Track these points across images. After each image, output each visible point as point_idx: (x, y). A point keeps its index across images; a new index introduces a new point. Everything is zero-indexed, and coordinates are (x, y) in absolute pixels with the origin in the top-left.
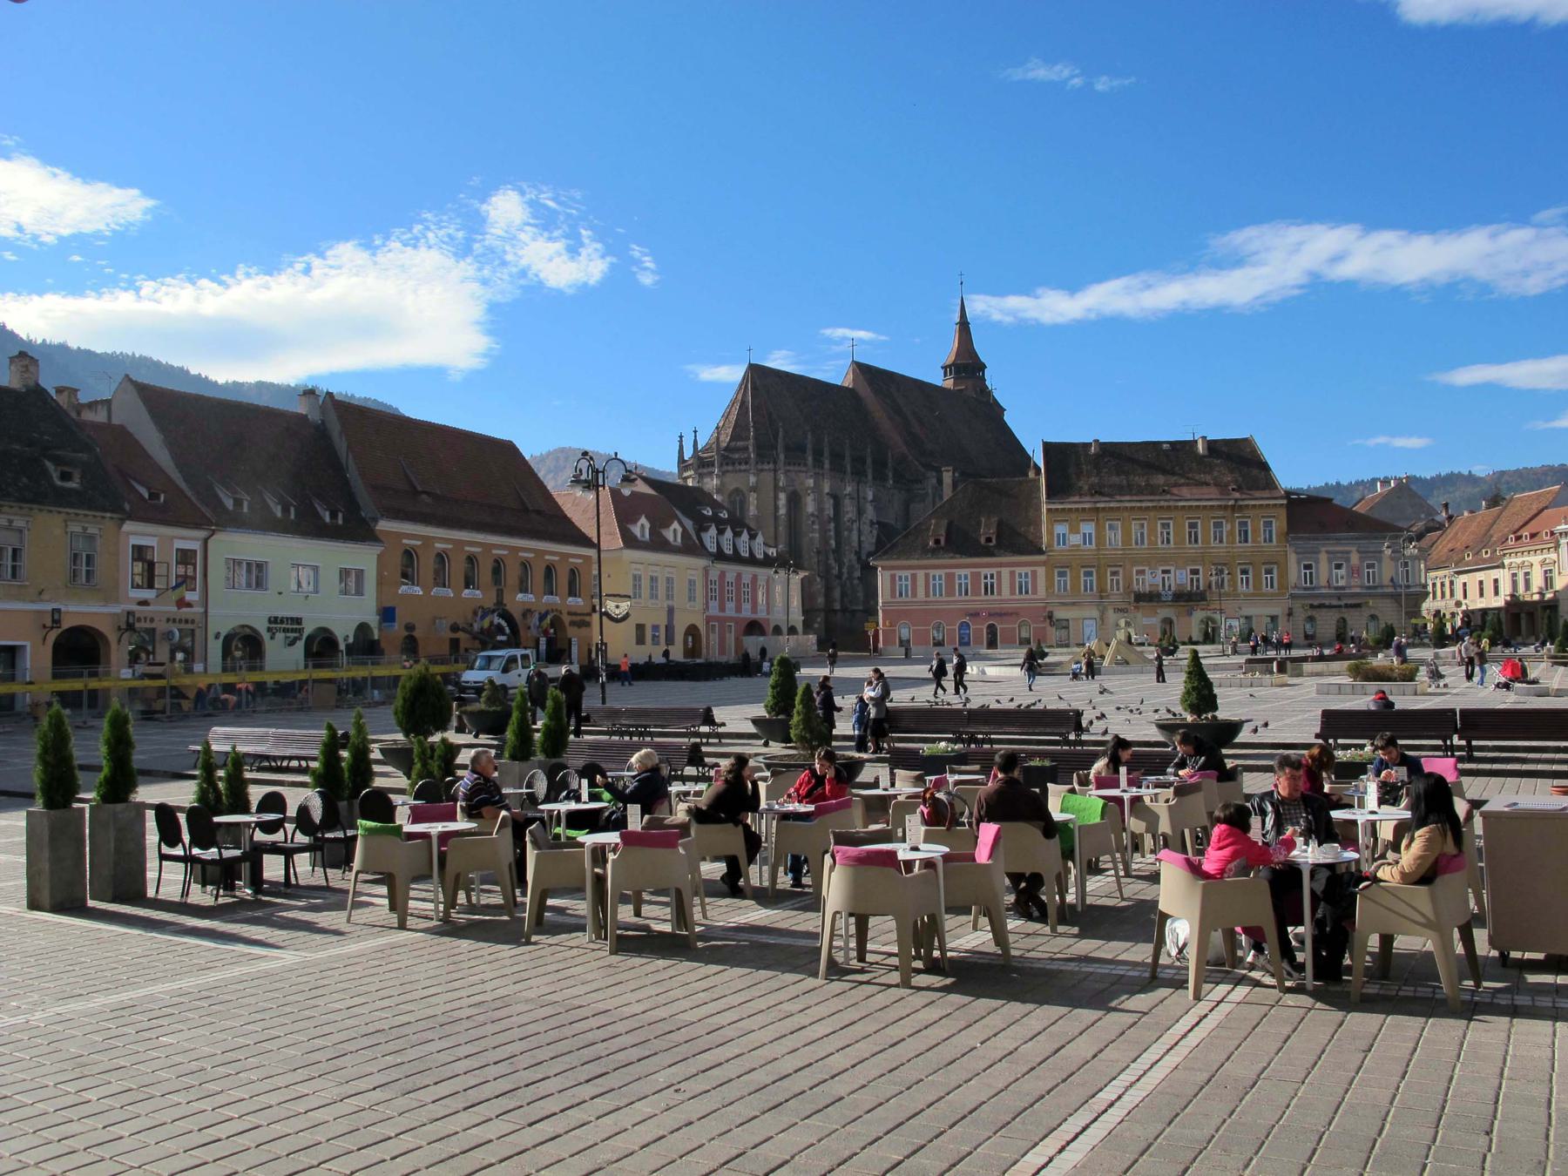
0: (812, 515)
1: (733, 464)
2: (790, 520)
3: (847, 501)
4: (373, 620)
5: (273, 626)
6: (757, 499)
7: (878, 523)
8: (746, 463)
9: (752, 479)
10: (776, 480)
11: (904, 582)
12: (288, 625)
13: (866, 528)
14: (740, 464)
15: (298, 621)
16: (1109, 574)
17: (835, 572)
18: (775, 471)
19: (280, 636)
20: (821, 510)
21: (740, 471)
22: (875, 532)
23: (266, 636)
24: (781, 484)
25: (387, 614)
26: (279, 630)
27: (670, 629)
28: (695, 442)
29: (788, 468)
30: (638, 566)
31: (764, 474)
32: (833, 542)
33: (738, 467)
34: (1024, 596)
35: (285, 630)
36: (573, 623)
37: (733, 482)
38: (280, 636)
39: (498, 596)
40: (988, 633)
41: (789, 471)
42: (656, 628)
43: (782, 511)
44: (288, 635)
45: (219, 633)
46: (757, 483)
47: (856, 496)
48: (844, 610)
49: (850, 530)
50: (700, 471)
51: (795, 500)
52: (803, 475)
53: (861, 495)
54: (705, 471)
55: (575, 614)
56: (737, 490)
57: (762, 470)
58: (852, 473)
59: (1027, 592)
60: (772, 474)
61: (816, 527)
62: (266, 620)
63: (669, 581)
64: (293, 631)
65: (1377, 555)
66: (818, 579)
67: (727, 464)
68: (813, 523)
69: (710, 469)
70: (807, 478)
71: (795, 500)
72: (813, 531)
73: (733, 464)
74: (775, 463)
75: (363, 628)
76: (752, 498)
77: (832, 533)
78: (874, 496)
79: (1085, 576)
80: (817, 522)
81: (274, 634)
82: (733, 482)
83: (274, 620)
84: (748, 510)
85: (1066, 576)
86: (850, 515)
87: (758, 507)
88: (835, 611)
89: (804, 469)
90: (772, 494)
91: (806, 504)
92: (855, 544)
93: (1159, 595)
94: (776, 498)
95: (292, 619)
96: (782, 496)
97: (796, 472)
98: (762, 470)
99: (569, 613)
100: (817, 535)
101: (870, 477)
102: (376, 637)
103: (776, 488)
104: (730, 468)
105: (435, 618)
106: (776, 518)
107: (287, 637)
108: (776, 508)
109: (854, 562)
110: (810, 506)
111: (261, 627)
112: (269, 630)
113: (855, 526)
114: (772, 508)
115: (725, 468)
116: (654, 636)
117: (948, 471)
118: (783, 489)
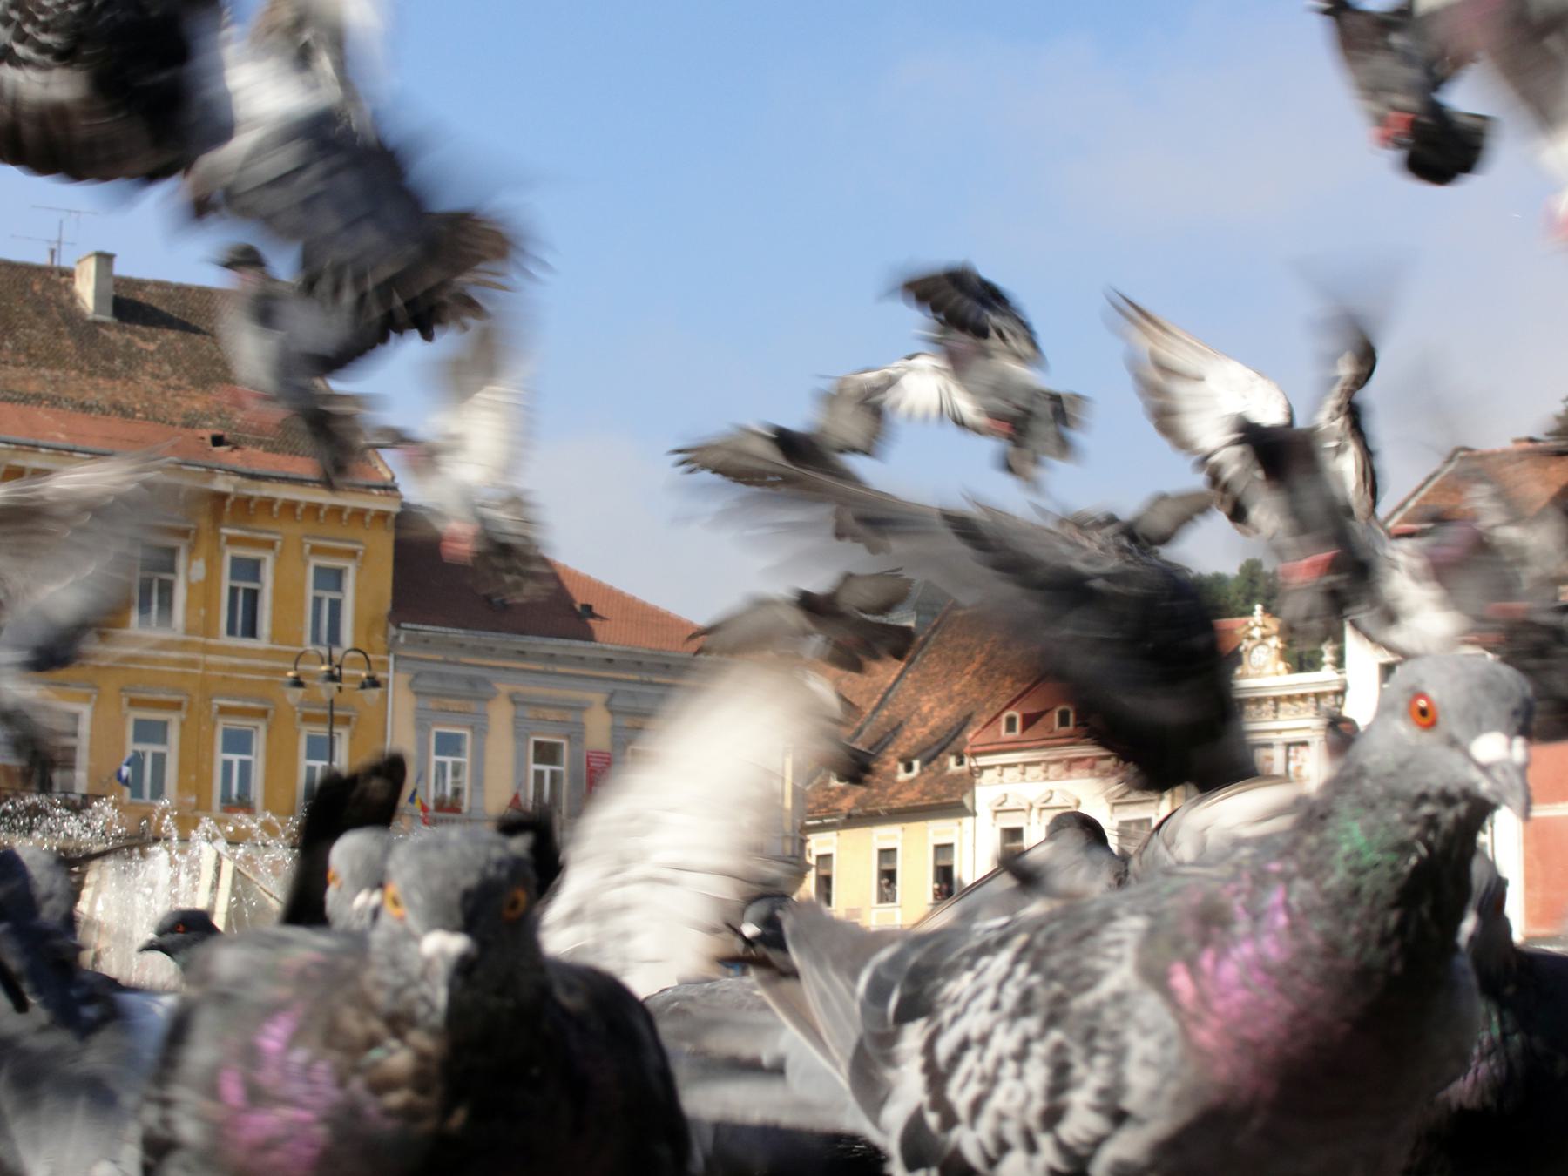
65: (571, 716)
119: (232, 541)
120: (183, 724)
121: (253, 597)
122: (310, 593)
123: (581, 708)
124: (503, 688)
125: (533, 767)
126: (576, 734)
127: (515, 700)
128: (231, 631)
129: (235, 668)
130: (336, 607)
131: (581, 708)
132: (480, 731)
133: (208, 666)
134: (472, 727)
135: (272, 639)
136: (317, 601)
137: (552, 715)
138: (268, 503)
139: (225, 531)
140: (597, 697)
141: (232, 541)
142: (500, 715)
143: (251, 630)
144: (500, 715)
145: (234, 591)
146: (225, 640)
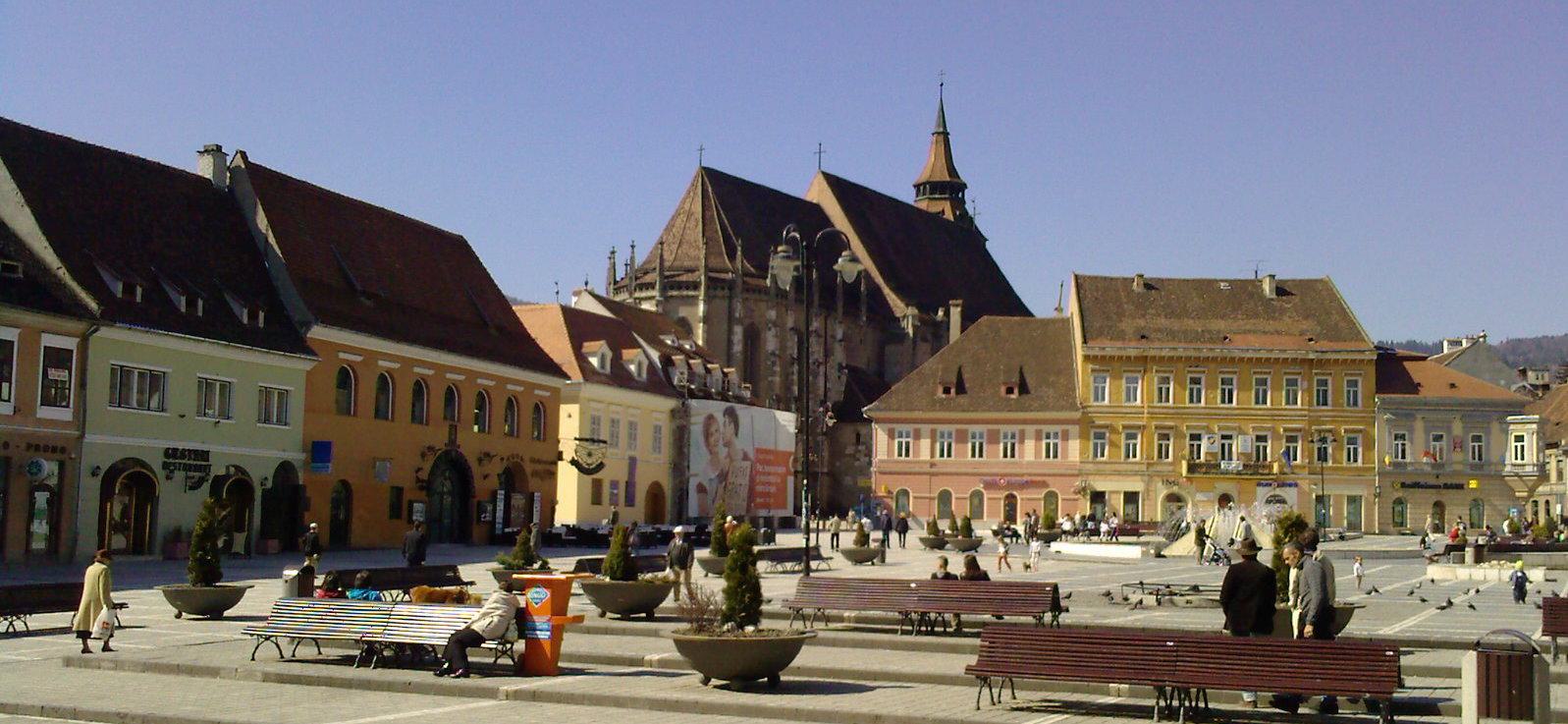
0: (773, 354)
2: (746, 358)
3: (813, 340)
4: (296, 456)
5: (171, 460)
7: (847, 367)
10: (731, 311)
12: (190, 463)
13: (833, 373)
15: (204, 455)
16: (1156, 437)
18: (730, 298)
19: (179, 475)
20: (783, 347)
22: (844, 378)
23: (161, 473)
24: (737, 315)
25: (320, 451)
26: (178, 467)
27: (630, 485)
29: (747, 296)
30: (619, 409)
31: (717, 301)
32: (796, 388)
33: (685, 293)
35: (187, 468)
36: (535, 474)
38: (179, 475)
39: (450, 434)
40: (1005, 506)
41: (747, 298)
42: (614, 485)
44: (191, 474)
45: (98, 467)
47: (822, 333)
49: (816, 377)
51: (753, 337)
52: (763, 305)
53: (829, 333)
55: (539, 461)
57: (715, 297)
58: (820, 306)
60: (726, 303)
61: (777, 369)
62: (162, 454)
63: (632, 425)
64: (198, 468)
68: (774, 364)
70: (768, 308)
71: (753, 337)
72: (774, 374)
75: (285, 469)
77: (795, 377)
78: (844, 333)
80: (778, 363)
81: (172, 472)
83: (171, 453)
85: (1136, 438)
86: (816, 356)
89: (765, 298)
90: (725, 326)
91: (765, 342)
92: (821, 391)
94: (730, 332)
95: (196, 452)
96: (738, 330)
97: (756, 300)
99: (533, 461)
100: (777, 379)
101: (840, 310)
102: (301, 483)
103: (731, 320)
105: (375, 460)
107: (187, 478)
108: (730, 343)
110: (770, 342)
111: (156, 462)
112: (165, 466)
113: (822, 369)
114: (724, 344)
116: (612, 494)
117: (957, 306)
118: (740, 321)
119: (1316, 374)
122: (1345, 389)
124: (1419, 416)
128: (1318, 404)
130: (1355, 393)
132: (1411, 430)
136: (1349, 392)
141: (1316, 374)
142: (1419, 425)
143: (1326, 404)
144: (1419, 425)
145: (1318, 391)
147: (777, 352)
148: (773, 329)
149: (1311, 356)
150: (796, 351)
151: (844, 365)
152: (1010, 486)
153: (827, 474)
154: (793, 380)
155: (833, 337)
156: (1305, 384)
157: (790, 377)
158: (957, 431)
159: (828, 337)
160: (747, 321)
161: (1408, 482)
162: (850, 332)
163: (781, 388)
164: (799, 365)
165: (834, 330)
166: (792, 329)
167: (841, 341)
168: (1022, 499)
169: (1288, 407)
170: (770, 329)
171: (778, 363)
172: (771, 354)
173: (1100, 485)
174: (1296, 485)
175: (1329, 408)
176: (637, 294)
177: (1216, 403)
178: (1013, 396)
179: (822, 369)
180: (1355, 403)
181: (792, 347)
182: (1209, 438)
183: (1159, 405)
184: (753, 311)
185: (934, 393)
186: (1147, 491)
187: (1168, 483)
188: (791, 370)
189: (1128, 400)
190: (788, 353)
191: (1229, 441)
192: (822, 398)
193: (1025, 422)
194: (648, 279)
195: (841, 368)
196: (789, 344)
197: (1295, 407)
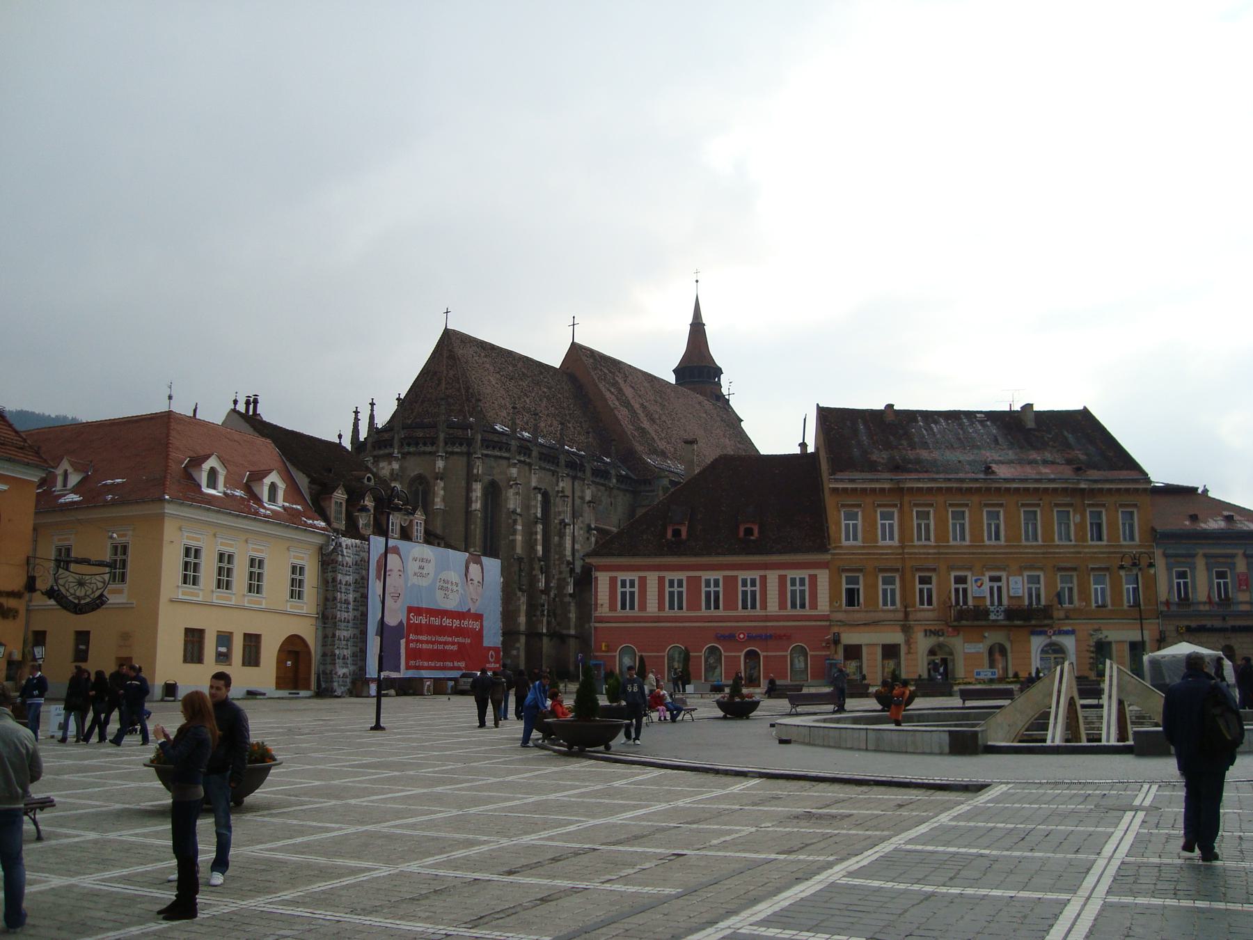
0: (514, 512)
1: (417, 444)
6: (444, 489)
8: (433, 444)
9: (440, 464)
11: (676, 589)
14: (425, 444)
17: (542, 585)
18: (469, 454)
21: (424, 453)
28: (372, 417)
32: (540, 548)
33: (423, 449)
34: (799, 612)
37: (415, 467)
43: (477, 506)
46: (445, 468)
48: (552, 635)
50: (375, 453)
51: (493, 492)
52: (504, 463)
54: (381, 452)
56: (420, 478)
57: (452, 453)
59: (803, 606)
65: (1229, 560)
66: (519, 594)
67: (409, 445)
69: (387, 451)
71: (493, 492)
73: (417, 444)
74: (469, 445)
76: (439, 489)
77: (539, 537)
79: (884, 583)
82: (415, 467)
84: (433, 503)
85: (893, 583)
87: (444, 499)
88: (540, 635)
91: (507, 499)
93: (986, 613)
94: (469, 490)
98: (452, 453)
104: (412, 449)
106: (468, 513)
108: (468, 501)
109: (566, 575)
115: (406, 449)
119: (1089, 505)
120: (1078, 576)
121: (1099, 526)
123: (1233, 556)
125: (1216, 581)
126: (1233, 566)
127: (1205, 556)
129: (1096, 553)
131: (1233, 556)
132: (1193, 568)
133: (1086, 553)
134: (1189, 568)
135: (1108, 541)
137: (1222, 560)
138: (1101, 490)
139: (1086, 502)
140: (1240, 552)
141: (1089, 505)
142: (1200, 564)
143: (1100, 539)
144: (1200, 564)
146: (1090, 543)
147: (519, 510)
148: (514, 487)
149: (1083, 486)
150: (539, 510)
151: (593, 526)
152: (751, 638)
153: (575, 637)
154: (536, 540)
155: (582, 498)
156: (1078, 518)
157: (534, 537)
158: (688, 578)
159: (576, 498)
160: (487, 479)
161: (1193, 624)
162: (600, 493)
163: (522, 548)
164: (543, 524)
165: (583, 491)
166: (535, 488)
167: (590, 502)
168: (764, 656)
169: (1061, 543)
170: (511, 486)
171: (520, 521)
172: (512, 512)
173: (849, 638)
174: (1073, 632)
175: (1104, 543)
176: (375, 453)
177: (983, 541)
178: (752, 538)
179: (568, 531)
180: (1132, 538)
181: (536, 507)
182: (976, 581)
183: (920, 543)
184: (494, 468)
185: (664, 534)
186: (908, 642)
187: (929, 633)
188: (534, 530)
189: (884, 538)
190: (533, 511)
191: (999, 584)
192: (570, 559)
193: (766, 567)
194: (386, 436)
195: (589, 529)
196: (533, 503)
197: (1069, 543)
